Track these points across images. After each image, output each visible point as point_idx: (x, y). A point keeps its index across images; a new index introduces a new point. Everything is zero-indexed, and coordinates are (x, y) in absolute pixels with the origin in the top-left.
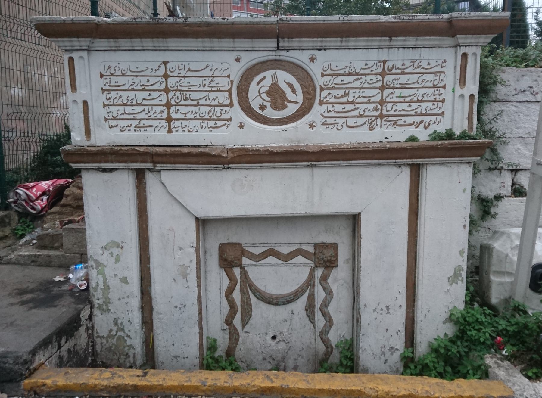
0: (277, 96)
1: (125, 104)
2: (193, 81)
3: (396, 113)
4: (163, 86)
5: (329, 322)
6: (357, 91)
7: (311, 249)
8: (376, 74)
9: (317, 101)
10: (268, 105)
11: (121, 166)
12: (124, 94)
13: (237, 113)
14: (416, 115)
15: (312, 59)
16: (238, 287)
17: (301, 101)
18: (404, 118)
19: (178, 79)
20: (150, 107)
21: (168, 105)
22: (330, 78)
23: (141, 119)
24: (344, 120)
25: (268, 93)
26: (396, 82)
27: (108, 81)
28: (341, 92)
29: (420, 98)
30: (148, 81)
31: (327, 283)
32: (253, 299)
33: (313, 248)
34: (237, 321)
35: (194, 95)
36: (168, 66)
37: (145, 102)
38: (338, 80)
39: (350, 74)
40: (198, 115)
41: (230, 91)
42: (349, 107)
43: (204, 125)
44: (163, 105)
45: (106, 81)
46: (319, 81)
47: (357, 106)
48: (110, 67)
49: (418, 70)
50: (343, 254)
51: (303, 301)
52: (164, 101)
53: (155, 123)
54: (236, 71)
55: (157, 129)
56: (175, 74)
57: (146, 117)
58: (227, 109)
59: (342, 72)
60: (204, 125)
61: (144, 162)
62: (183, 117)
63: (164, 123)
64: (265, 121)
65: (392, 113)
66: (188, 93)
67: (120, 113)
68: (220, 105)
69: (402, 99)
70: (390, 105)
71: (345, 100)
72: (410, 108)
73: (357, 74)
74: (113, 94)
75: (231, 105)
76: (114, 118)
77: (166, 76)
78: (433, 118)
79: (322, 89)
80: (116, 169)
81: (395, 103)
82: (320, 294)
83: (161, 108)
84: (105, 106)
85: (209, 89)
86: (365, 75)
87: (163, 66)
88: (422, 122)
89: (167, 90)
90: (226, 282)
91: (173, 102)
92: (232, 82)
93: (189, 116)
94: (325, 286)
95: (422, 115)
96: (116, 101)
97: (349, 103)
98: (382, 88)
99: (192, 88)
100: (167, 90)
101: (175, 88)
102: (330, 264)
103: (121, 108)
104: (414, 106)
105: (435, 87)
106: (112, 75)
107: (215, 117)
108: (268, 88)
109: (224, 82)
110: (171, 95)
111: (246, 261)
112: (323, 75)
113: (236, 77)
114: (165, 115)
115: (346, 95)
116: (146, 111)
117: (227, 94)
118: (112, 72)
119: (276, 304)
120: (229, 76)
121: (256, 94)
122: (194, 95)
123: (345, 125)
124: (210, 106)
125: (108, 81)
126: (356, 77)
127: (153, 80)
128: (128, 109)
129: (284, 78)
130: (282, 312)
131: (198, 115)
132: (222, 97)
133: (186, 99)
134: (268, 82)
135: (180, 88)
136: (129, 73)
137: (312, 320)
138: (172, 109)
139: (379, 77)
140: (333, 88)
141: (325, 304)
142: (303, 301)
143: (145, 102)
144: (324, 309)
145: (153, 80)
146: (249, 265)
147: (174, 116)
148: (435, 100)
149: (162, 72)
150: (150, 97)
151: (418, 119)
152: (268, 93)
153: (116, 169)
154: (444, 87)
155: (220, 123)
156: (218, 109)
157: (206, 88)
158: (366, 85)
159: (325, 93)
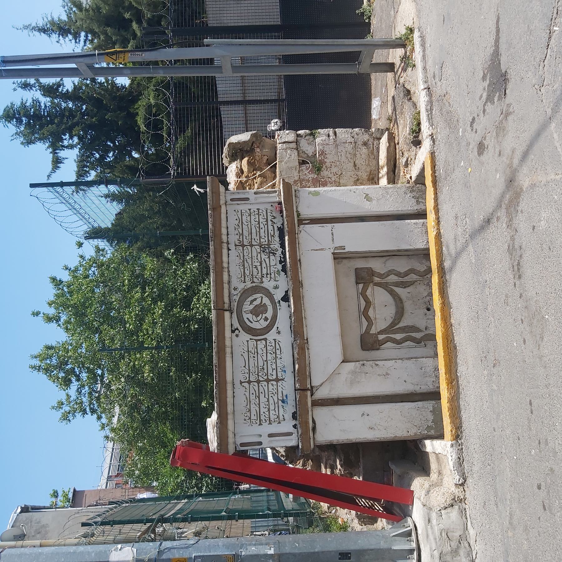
0: (258, 311)
1: (269, 410)
2: (252, 365)
3: (266, 236)
4: (256, 384)
5: (412, 271)
6: (253, 260)
7: (361, 286)
8: (243, 250)
9: (260, 285)
10: (264, 316)
11: (310, 413)
12: (262, 410)
13: (271, 336)
14: (267, 224)
15: (235, 289)
16: (392, 336)
17: (261, 295)
18: (270, 231)
19: (251, 374)
20: (270, 393)
21: (268, 381)
22: (246, 277)
23: (278, 399)
24: (272, 267)
25: (257, 316)
26: (248, 238)
27: (254, 421)
28: (255, 270)
29: (257, 223)
30: (253, 394)
31: (384, 274)
32: (401, 325)
33: (360, 285)
34: (418, 335)
35: (261, 364)
36: (243, 381)
37: (267, 396)
38: (247, 272)
39: (244, 266)
40: (273, 361)
41: (257, 341)
42: (264, 265)
43: (279, 357)
44: (268, 384)
45: (254, 422)
46: (249, 285)
47: (263, 260)
48: (245, 420)
49: (240, 225)
50: (361, 264)
51: (398, 290)
52: (266, 383)
53: (280, 390)
54: (244, 336)
55: (284, 388)
56: (247, 376)
57: (276, 395)
58: (268, 342)
59: (242, 271)
60: (279, 357)
61: (307, 399)
62: (275, 371)
63: (279, 384)
64: (275, 317)
65: (266, 239)
66: (259, 368)
67: (274, 413)
68: (266, 346)
69: (258, 233)
70: (262, 240)
71: (259, 268)
72: (263, 228)
73: (243, 261)
74: (263, 418)
75: (265, 339)
76: (278, 417)
77: (249, 382)
78: (269, 214)
79: (253, 282)
80: (313, 419)
81: (260, 237)
82: (393, 278)
83: (270, 385)
84: (270, 423)
85: (256, 353)
86: (244, 256)
87: (243, 384)
88: (271, 220)
89: (258, 382)
90: (389, 344)
91: (266, 378)
92: (251, 339)
93: (274, 367)
94: (386, 275)
95: (267, 221)
96: (267, 416)
97: (261, 265)
98: (252, 246)
99: (256, 365)
100: (258, 382)
101: (257, 376)
102: (371, 272)
103: (271, 412)
104: (262, 226)
105: (250, 215)
106: (250, 418)
107: (274, 350)
108: (254, 316)
109: (252, 344)
110: (261, 379)
111: (373, 331)
112: (245, 282)
113: (248, 337)
114: (274, 383)
115: (256, 267)
116: (272, 395)
117: (259, 342)
118: (248, 418)
119: (403, 308)
120: (248, 341)
121: (260, 324)
122: (261, 364)
123: (275, 267)
124: (267, 353)
125: (254, 421)
126: (245, 262)
127: (252, 391)
128: (272, 407)
129: (247, 307)
130: (408, 305)
131: (273, 361)
132: (261, 345)
133: (263, 369)
134: (250, 316)
135: (256, 373)
136: (248, 406)
137: (412, 283)
138: (270, 378)
139: (245, 248)
140: (252, 275)
141: (398, 274)
142: (398, 290)
143: (267, 396)
144: (402, 275)
145: (252, 391)
146: (376, 329)
147: (274, 377)
148: (258, 214)
149: (246, 385)
150: (263, 392)
151: (270, 223)
152: (257, 316)
153: (313, 419)
154: (250, 210)
155: (278, 347)
156: (269, 348)
157: (256, 355)
158: (250, 255)
159: (255, 280)
